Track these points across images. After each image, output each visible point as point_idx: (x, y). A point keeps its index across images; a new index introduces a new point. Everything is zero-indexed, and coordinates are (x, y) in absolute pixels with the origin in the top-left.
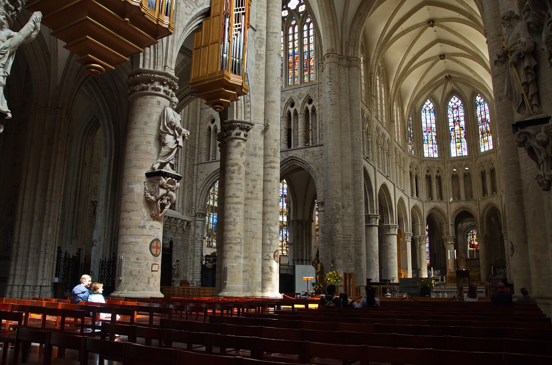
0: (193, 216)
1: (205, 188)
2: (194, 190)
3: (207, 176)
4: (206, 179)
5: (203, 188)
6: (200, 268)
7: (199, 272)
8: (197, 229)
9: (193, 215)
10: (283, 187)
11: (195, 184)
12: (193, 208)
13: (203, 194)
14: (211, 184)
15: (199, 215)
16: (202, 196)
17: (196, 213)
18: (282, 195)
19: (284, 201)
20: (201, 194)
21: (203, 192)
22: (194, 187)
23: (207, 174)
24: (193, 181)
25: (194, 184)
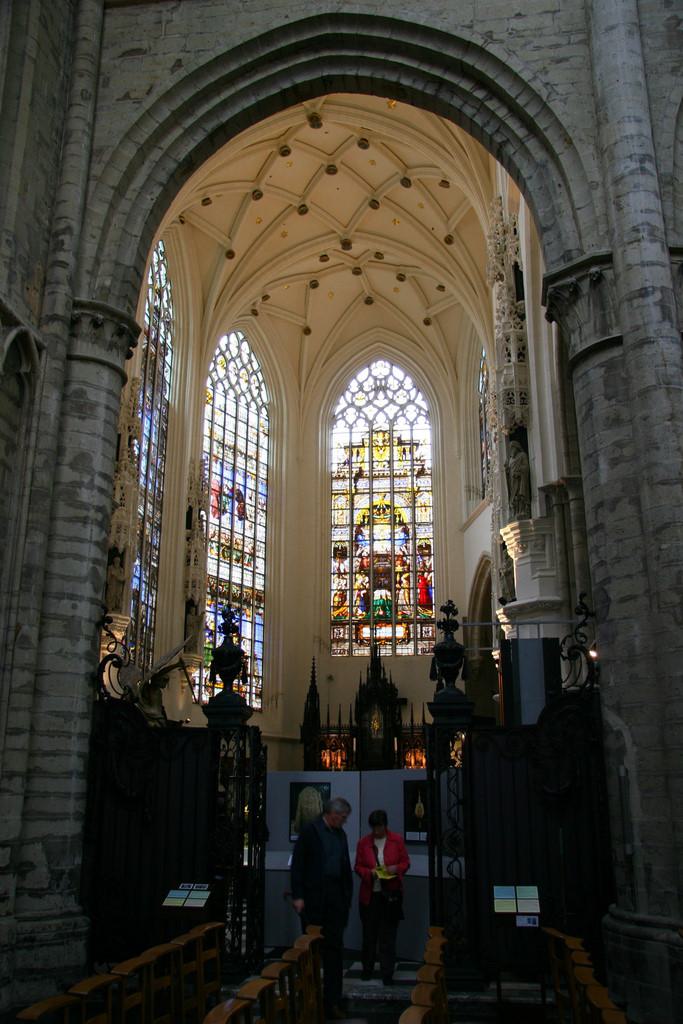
0: (54, 318)
1: (156, 155)
2: (78, 149)
3: (182, 73)
4: (168, 95)
5: (143, 151)
6: (84, 726)
7: (75, 763)
8: (73, 422)
9: (60, 310)
10: (234, 465)
11: (82, 111)
12: (64, 264)
13: (130, 194)
14: (200, 137)
15: (96, 324)
16: (124, 206)
17: (77, 305)
18: (232, 490)
19: (236, 512)
20: (120, 191)
21: (139, 180)
22: (78, 126)
23: (179, 64)
24: (67, 87)
25: (76, 111)
